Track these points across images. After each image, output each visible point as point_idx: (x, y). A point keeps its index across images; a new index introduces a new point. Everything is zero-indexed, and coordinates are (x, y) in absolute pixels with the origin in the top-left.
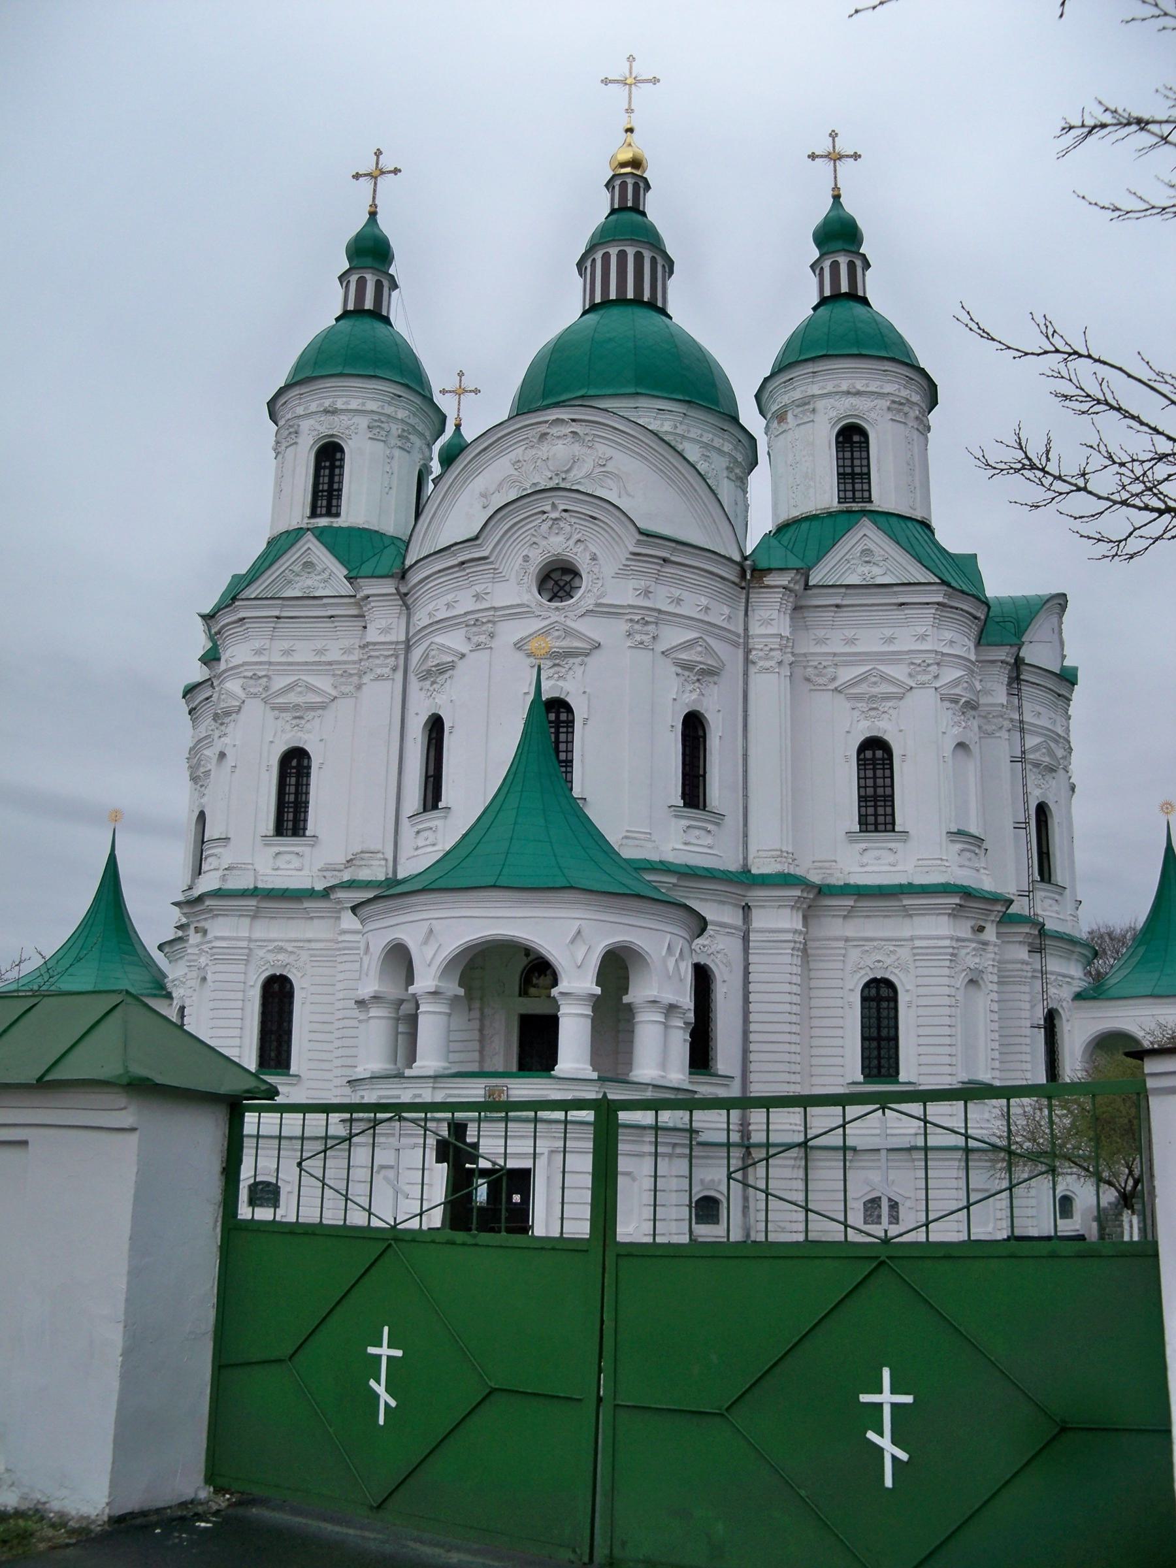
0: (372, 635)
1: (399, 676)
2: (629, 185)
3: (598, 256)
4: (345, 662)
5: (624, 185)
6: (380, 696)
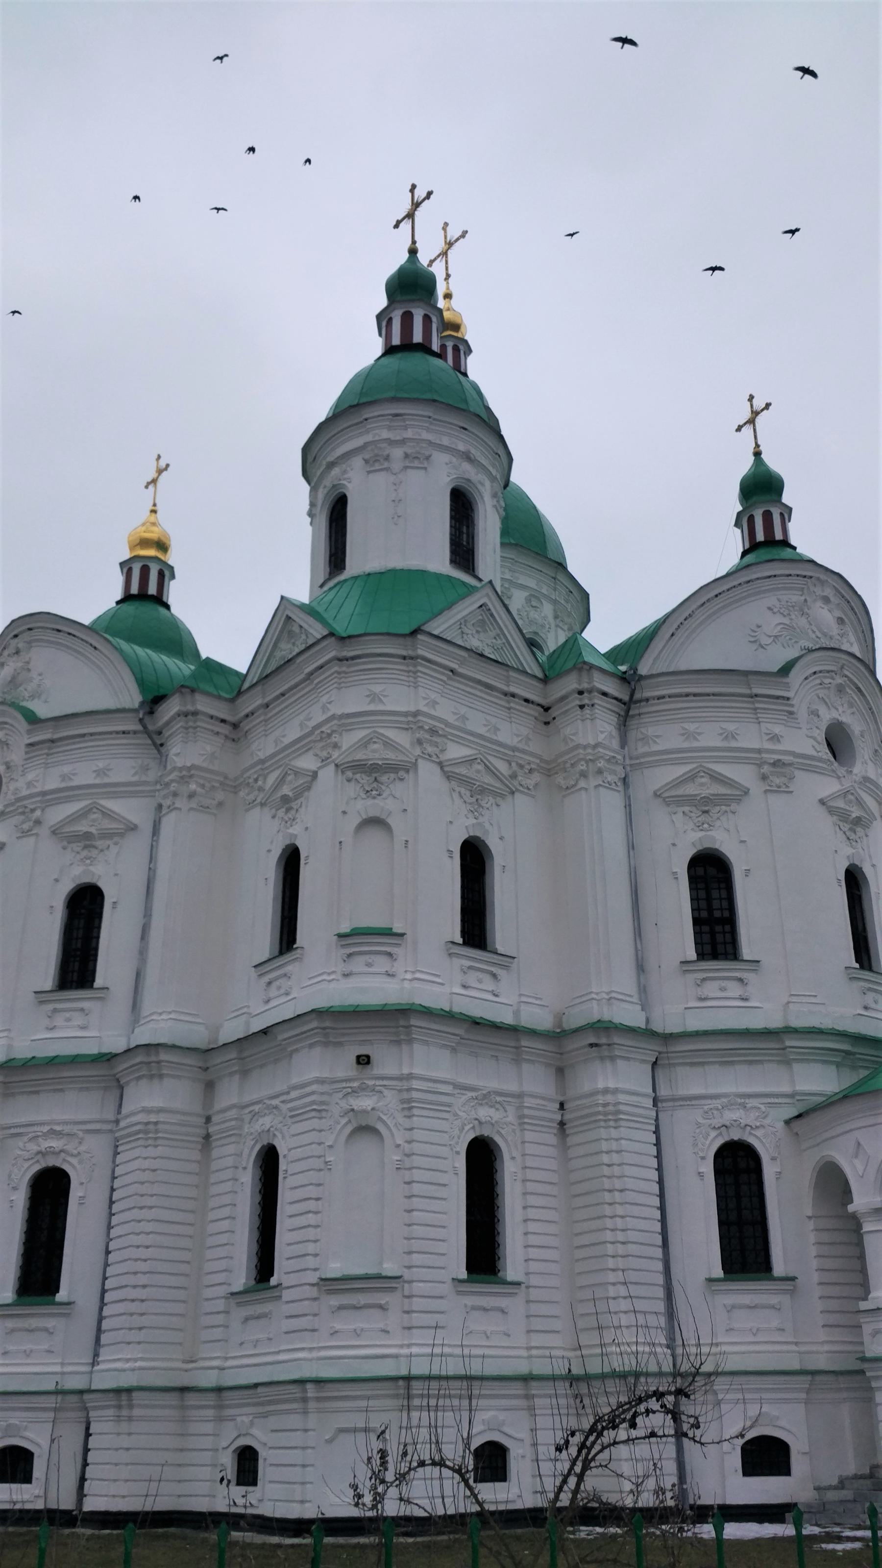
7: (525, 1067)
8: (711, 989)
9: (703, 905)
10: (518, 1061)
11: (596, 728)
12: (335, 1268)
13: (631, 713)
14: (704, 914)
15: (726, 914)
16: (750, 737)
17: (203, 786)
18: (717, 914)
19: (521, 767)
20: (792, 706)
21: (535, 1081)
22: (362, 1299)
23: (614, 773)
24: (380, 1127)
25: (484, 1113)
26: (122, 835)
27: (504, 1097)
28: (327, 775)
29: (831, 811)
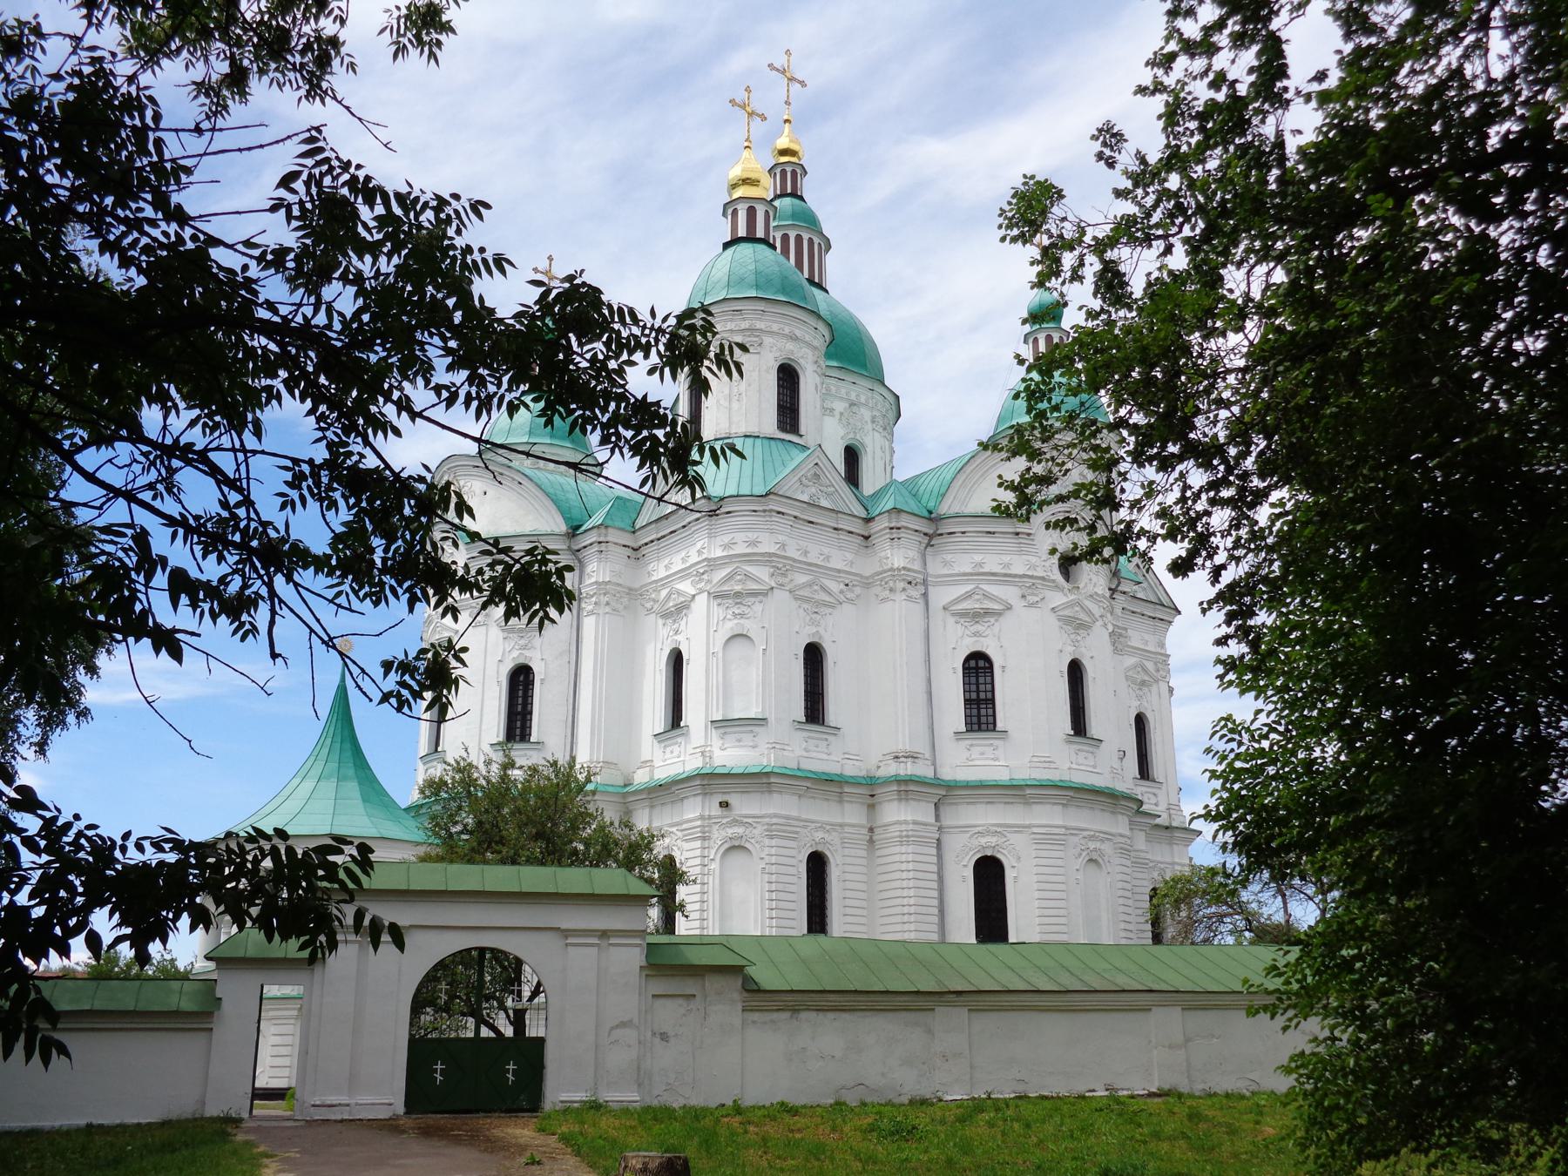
7: (847, 805)
8: (976, 751)
9: (974, 688)
10: (841, 801)
14: (974, 696)
15: (989, 695)
18: (982, 696)
21: (853, 815)
25: (819, 835)
27: (830, 825)
28: (702, 600)
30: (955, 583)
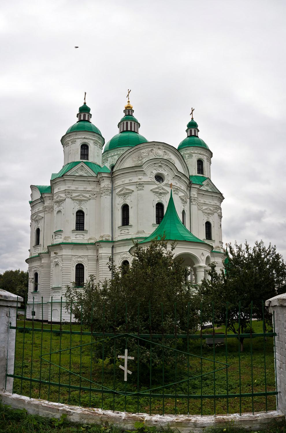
0: (103, 185)
1: (111, 195)
2: (129, 111)
3: (125, 122)
4: (93, 191)
5: (129, 111)
6: (106, 200)
11: (106, 183)
12: (54, 286)
13: (113, 179)
16: (135, 179)
17: (48, 209)
19: (92, 194)
20: (145, 172)
22: (56, 291)
23: (109, 192)
24: (59, 264)
26: (41, 219)
29: (154, 192)
30: (120, 187)
